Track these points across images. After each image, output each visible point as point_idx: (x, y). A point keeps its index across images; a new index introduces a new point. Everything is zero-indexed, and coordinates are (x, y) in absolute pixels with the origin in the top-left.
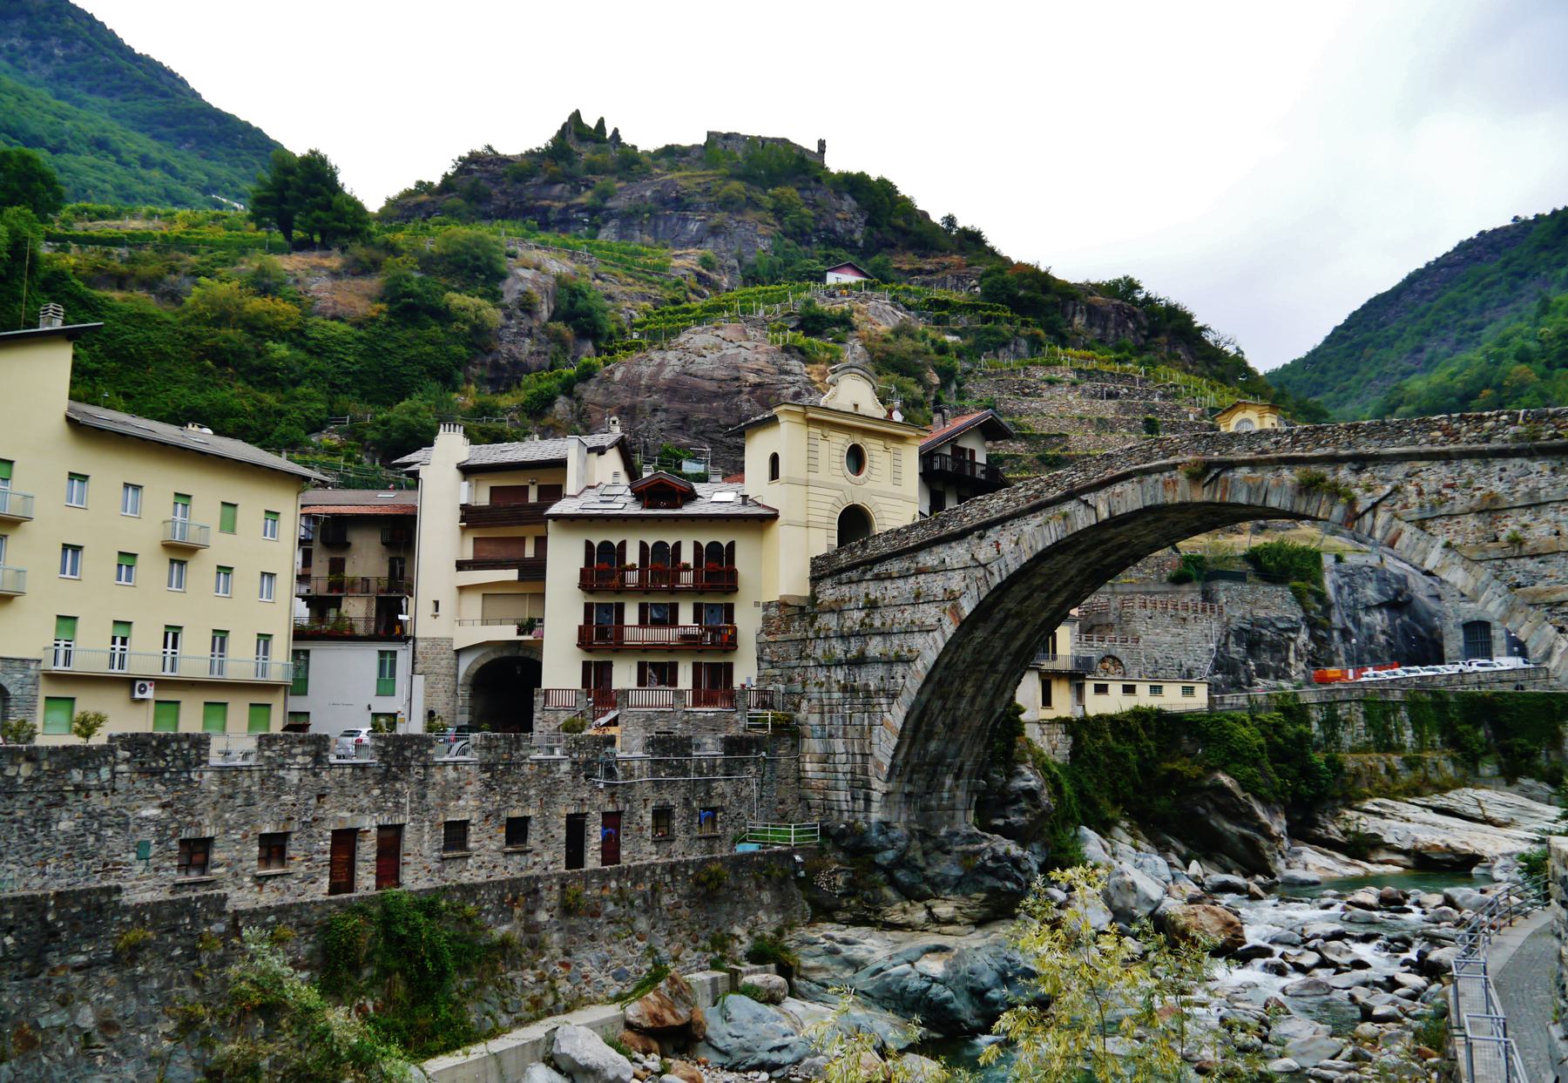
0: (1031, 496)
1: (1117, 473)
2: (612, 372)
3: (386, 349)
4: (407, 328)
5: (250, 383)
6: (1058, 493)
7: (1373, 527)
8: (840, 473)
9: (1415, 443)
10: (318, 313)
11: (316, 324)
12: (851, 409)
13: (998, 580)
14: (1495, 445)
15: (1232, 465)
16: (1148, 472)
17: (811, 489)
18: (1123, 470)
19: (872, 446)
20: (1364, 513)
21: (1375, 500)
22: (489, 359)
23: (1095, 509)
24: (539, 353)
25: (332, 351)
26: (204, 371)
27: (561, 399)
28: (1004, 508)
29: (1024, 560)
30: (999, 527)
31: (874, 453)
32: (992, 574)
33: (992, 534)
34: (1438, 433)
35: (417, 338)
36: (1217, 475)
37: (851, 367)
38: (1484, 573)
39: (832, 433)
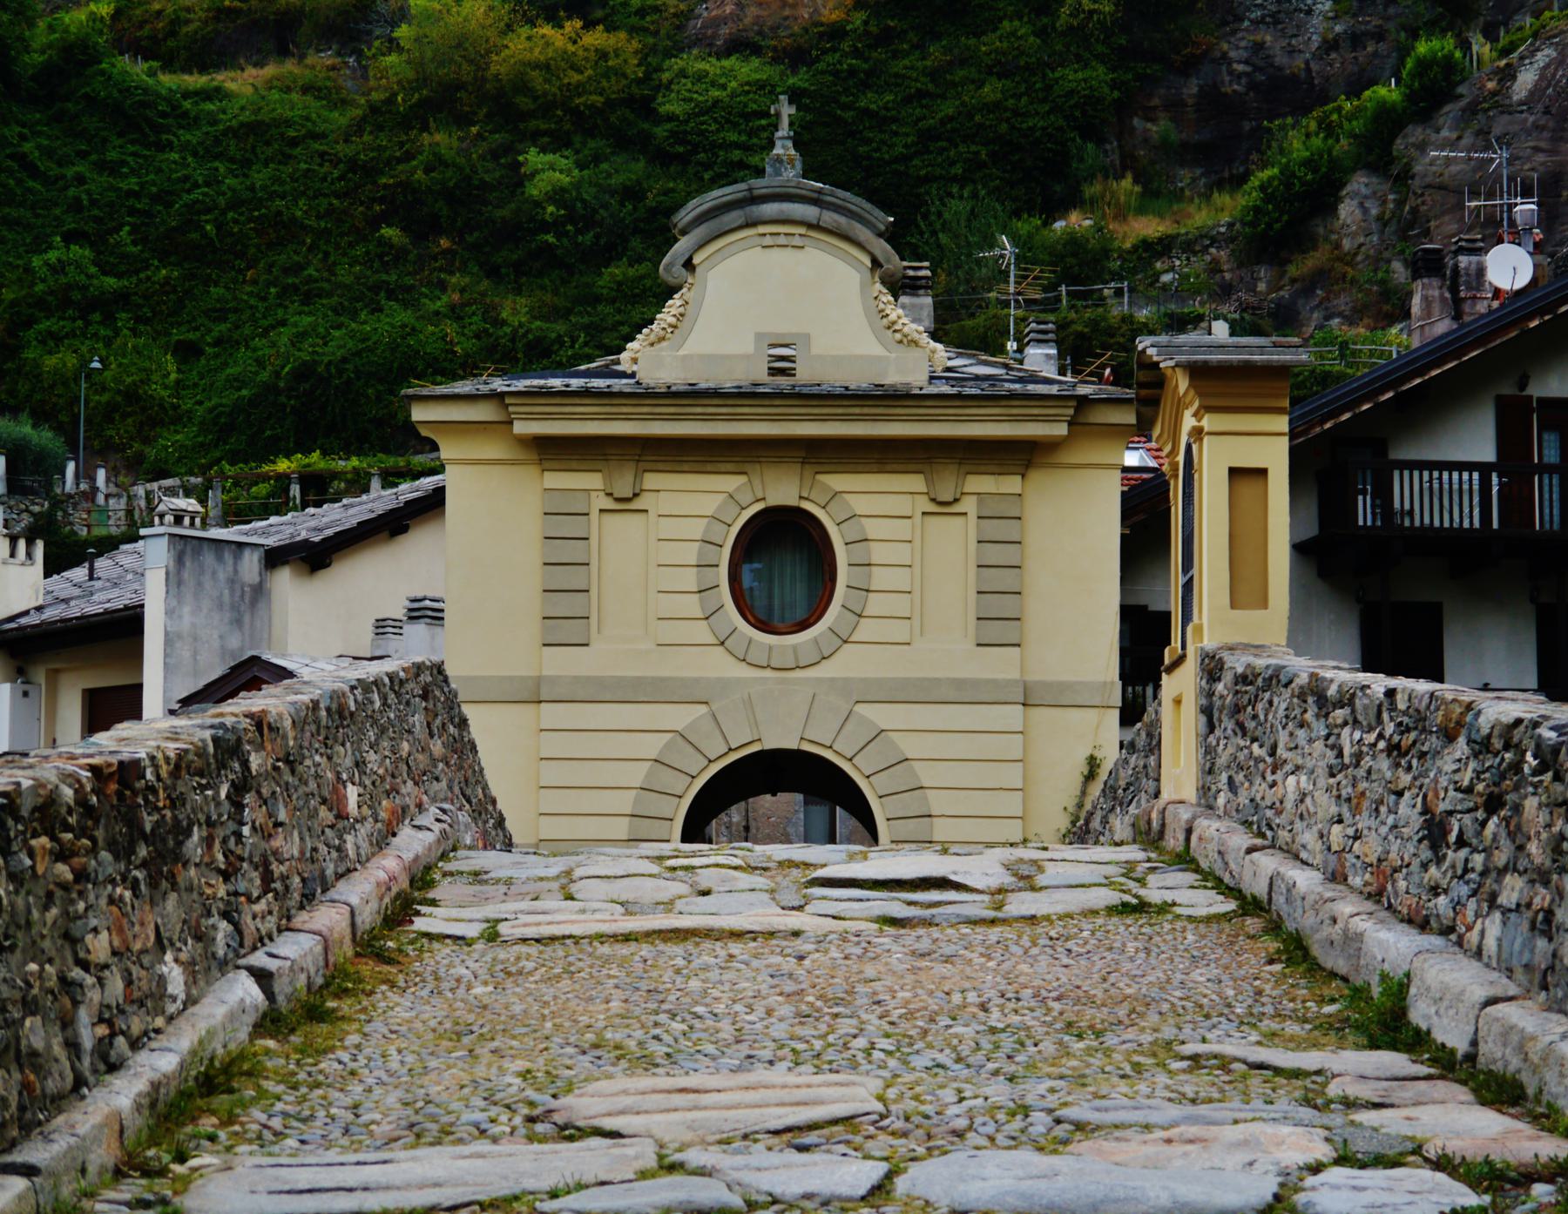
2: (1508, 74)
3: (866, 112)
4: (937, 37)
5: (493, 272)
8: (702, 632)
10: (697, 41)
11: (683, 73)
12: (756, 372)
17: (552, 714)
19: (860, 505)
22: (1192, 88)
24: (1356, 40)
25: (714, 147)
26: (391, 256)
27: (1360, 183)
31: (873, 528)
35: (963, 62)
37: (754, 199)
39: (651, 480)
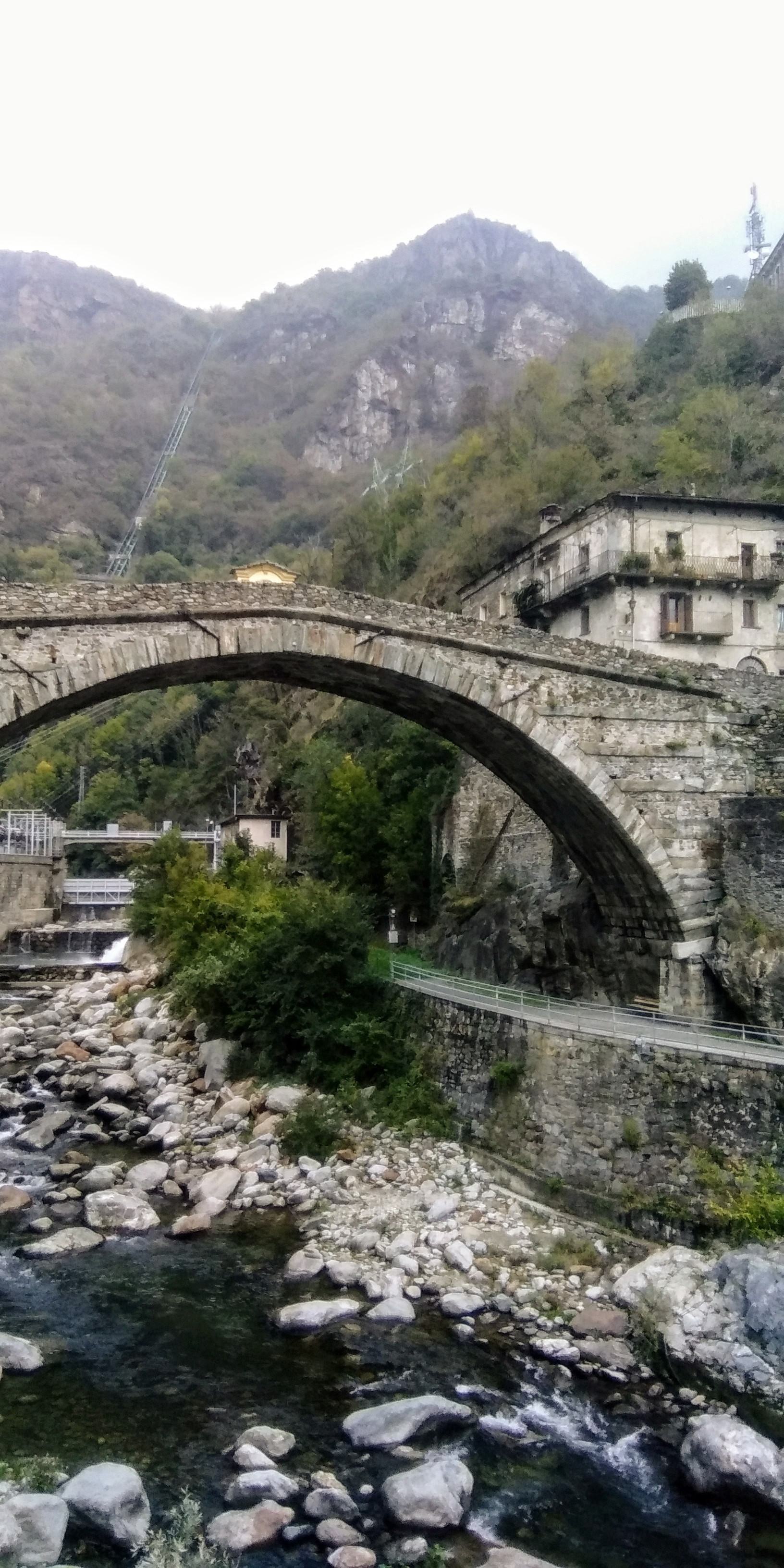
0: (118, 603)
1: (247, 607)
6: (160, 610)
7: (514, 714)
9: (551, 653)
13: (54, 695)
14: (608, 669)
15: (388, 632)
16: (289, 616)
18: (256, 606)
20: (506, 703)
21: (517, 693)
23: (218, 640)
28: (69, 608)
29: (103, 677)
30: (58, 629)
32: (43, 685)
33: (42, 635)
34: (569, 650)
36: (370, 639)
38: (595, 764)
